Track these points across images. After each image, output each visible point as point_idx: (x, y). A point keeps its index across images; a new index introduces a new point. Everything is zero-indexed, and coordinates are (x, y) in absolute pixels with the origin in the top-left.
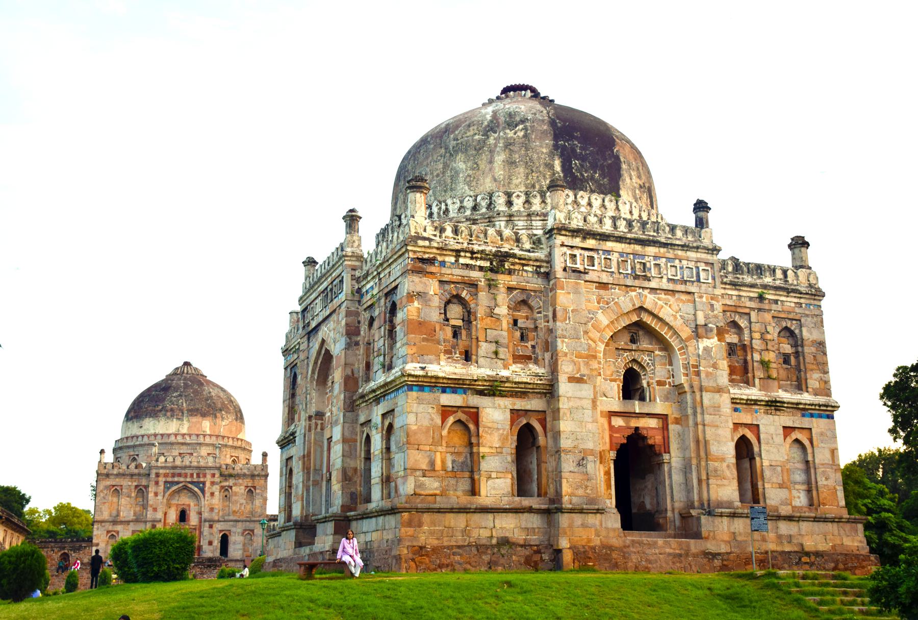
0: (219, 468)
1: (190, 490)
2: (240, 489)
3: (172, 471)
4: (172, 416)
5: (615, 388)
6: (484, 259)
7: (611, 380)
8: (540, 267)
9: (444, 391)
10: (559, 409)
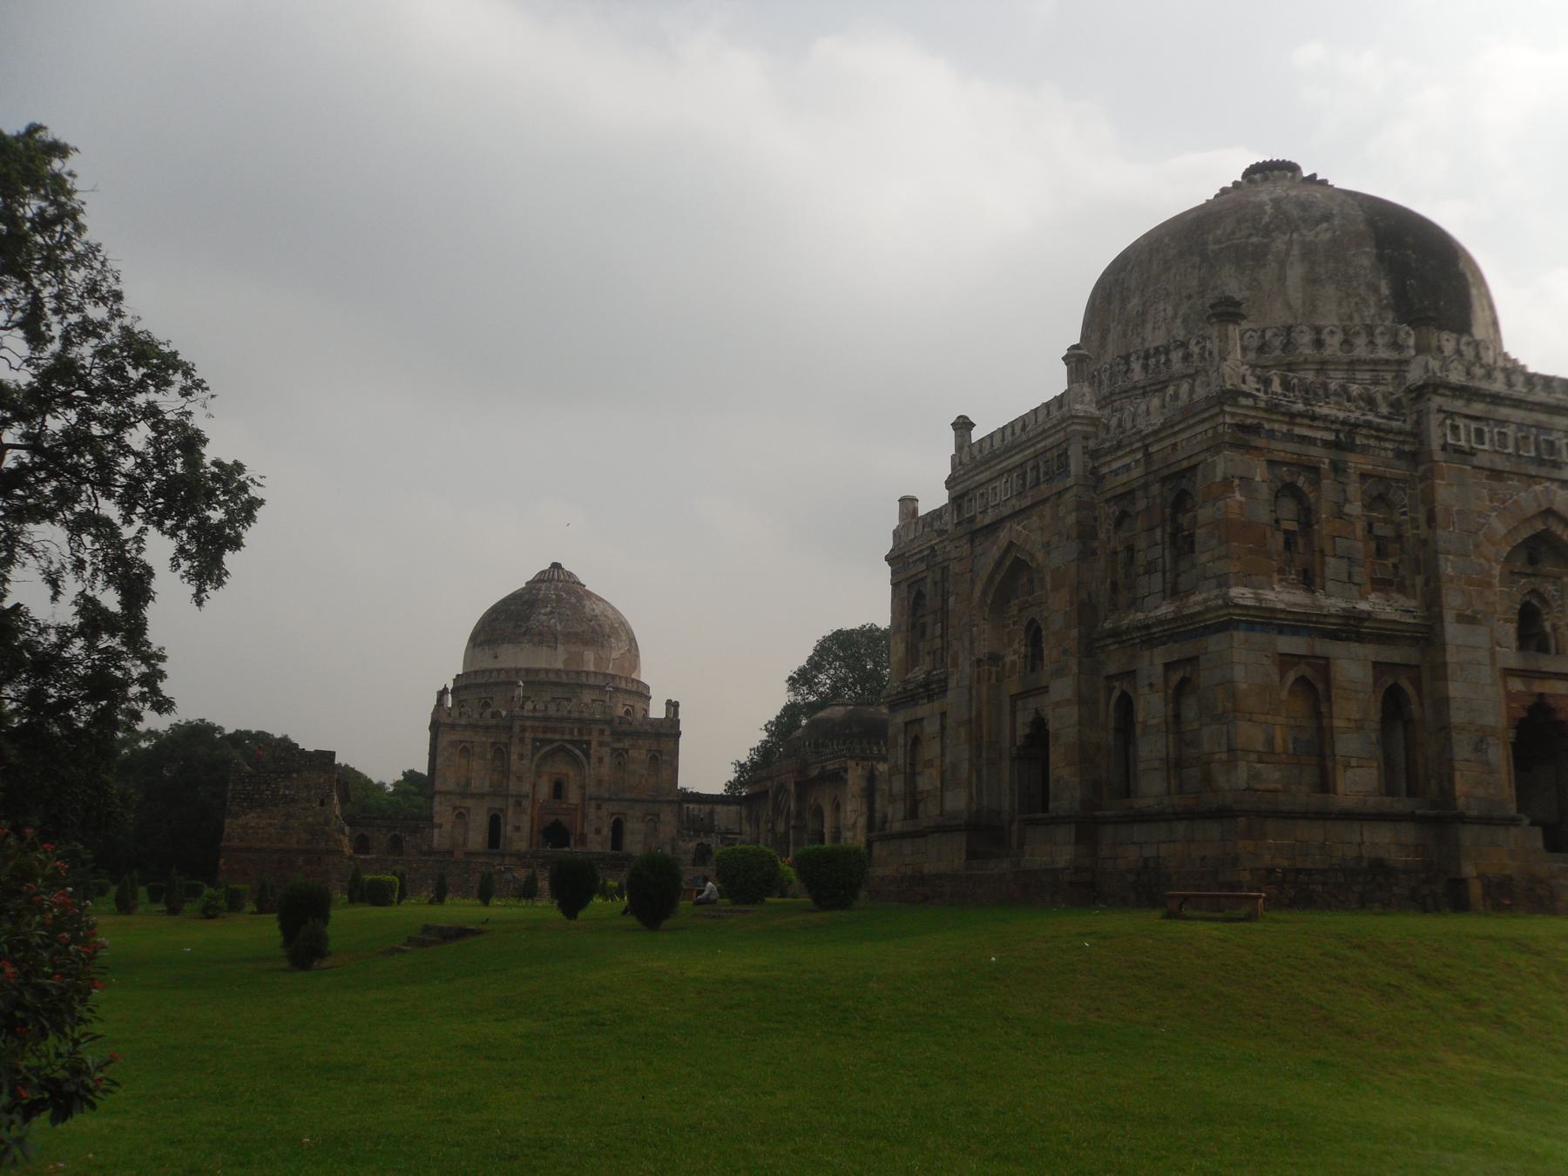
1: (569, 753)
4: (541, 643)
5: (1511, 630)
6: (1327, 429)
7: (1506, 621)
8: (1403, 442)
9: (1281, 632)
10: (1444, 664)
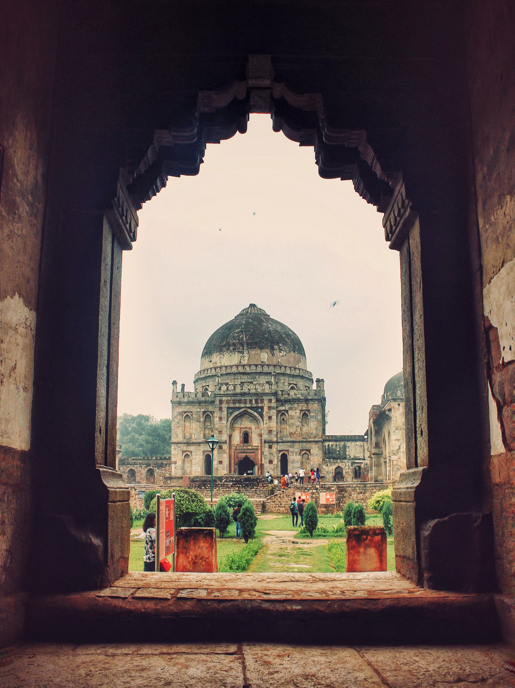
0: (275, 394)
1: (251, 415)
2: (295, 413)
3: (233, 398)
